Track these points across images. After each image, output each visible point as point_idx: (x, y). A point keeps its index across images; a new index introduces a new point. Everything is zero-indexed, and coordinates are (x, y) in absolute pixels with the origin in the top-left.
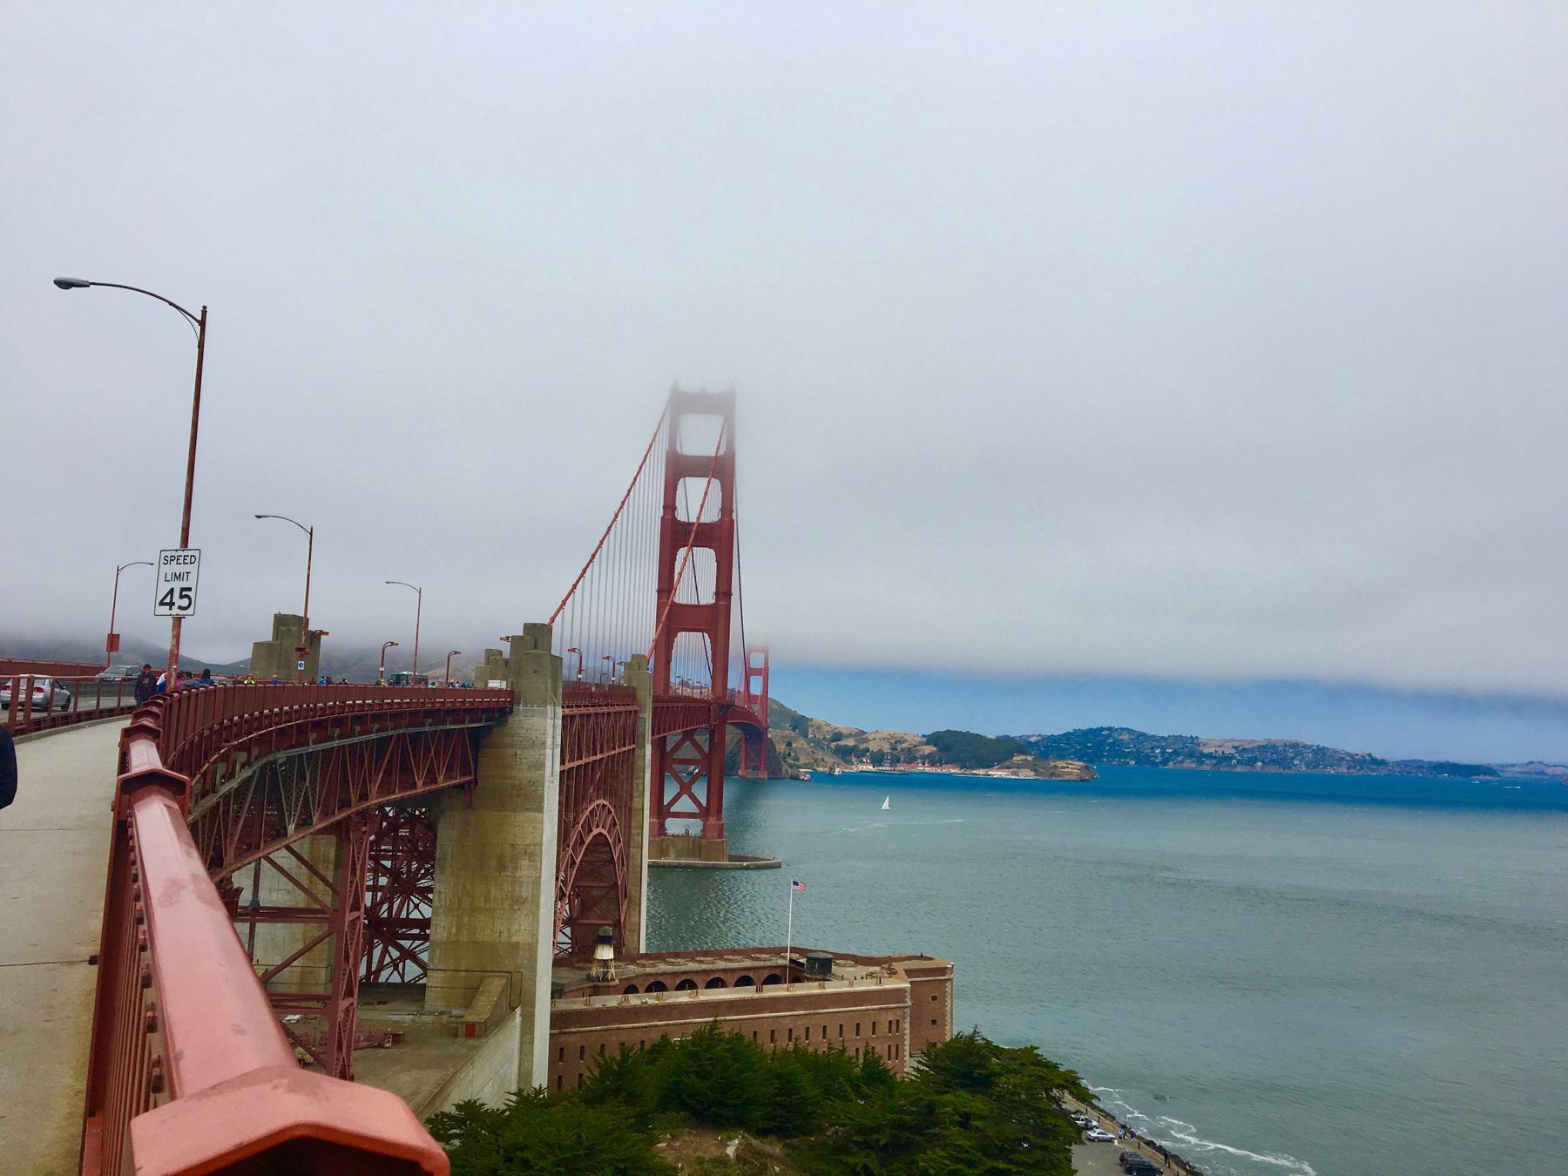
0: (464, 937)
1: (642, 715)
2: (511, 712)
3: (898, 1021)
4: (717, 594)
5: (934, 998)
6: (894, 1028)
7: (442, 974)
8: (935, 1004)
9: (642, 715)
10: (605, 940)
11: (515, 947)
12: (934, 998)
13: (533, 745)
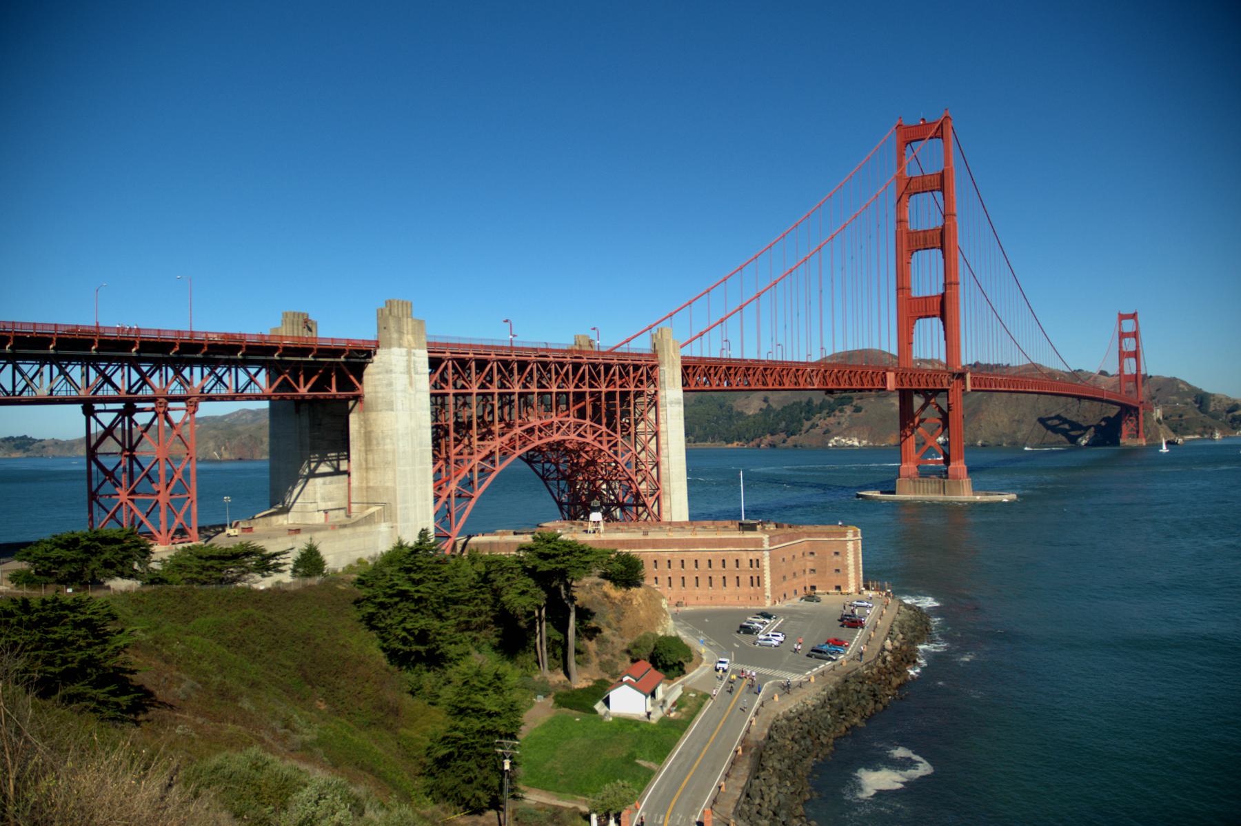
0: (364, 485)
1: (662, 368)
2: (375, 354)
3: (758, 560)
4: (945, 285)
5: (837, 553)
6: (755, 564)
7: (356, 505)
8: (839, 558)
9: (662, 368)
10: (596, 509)
11: (387, 488)
12: (837, 553)
13: (387, 372)
